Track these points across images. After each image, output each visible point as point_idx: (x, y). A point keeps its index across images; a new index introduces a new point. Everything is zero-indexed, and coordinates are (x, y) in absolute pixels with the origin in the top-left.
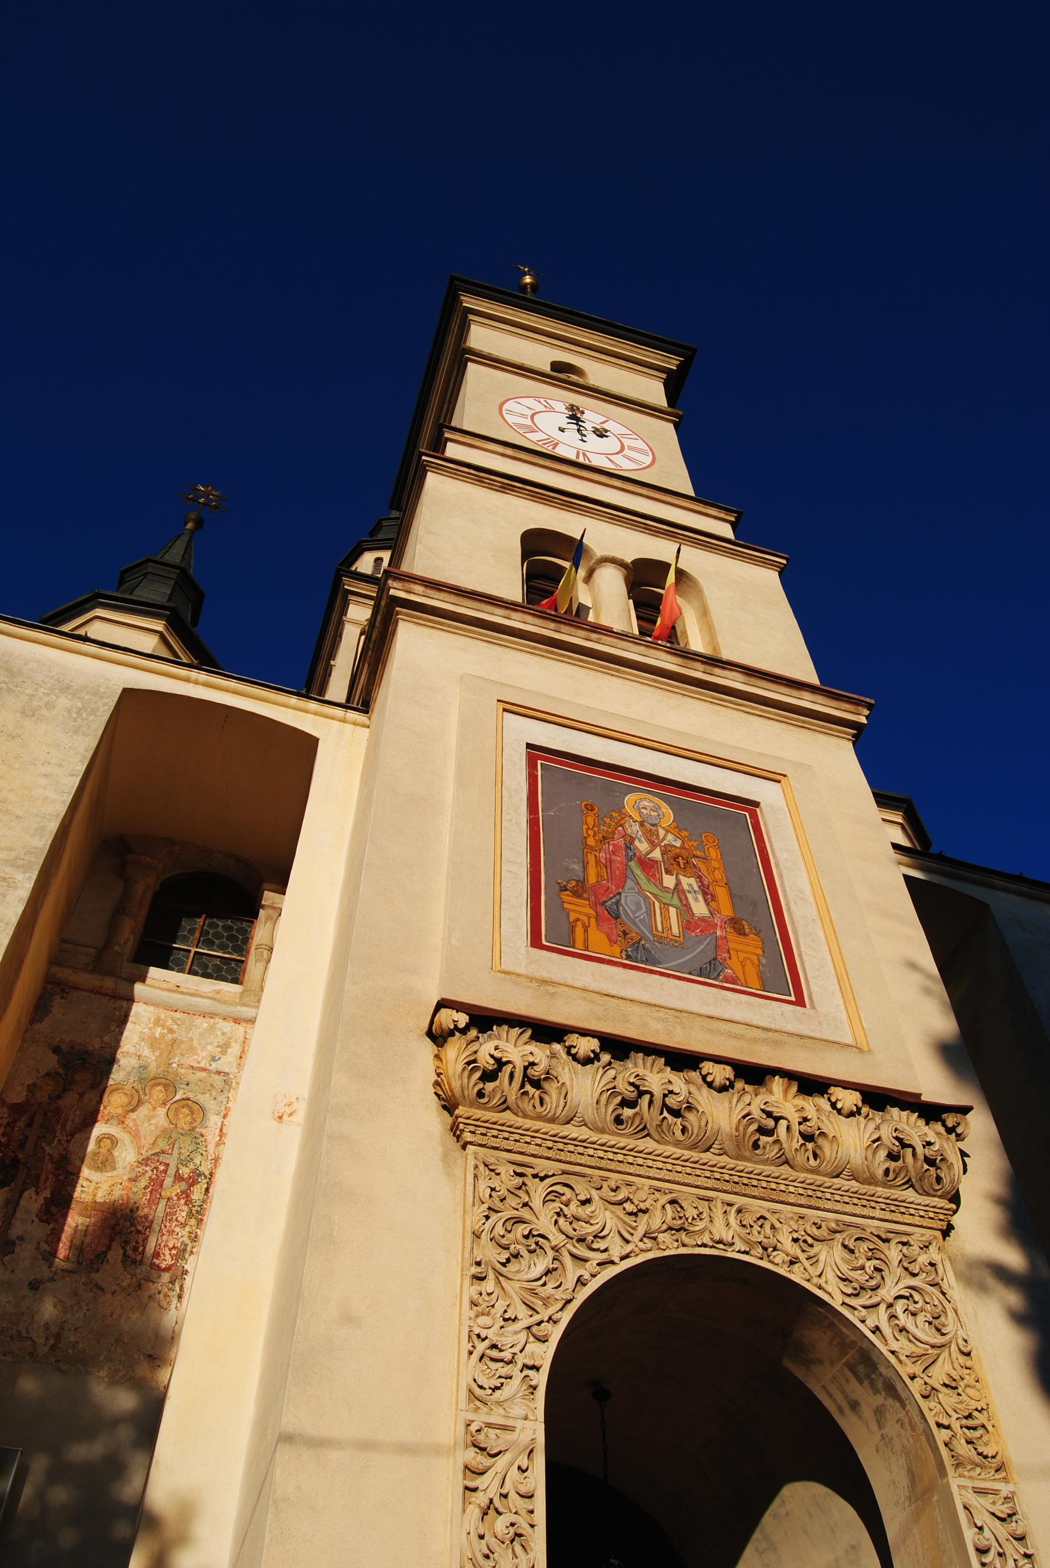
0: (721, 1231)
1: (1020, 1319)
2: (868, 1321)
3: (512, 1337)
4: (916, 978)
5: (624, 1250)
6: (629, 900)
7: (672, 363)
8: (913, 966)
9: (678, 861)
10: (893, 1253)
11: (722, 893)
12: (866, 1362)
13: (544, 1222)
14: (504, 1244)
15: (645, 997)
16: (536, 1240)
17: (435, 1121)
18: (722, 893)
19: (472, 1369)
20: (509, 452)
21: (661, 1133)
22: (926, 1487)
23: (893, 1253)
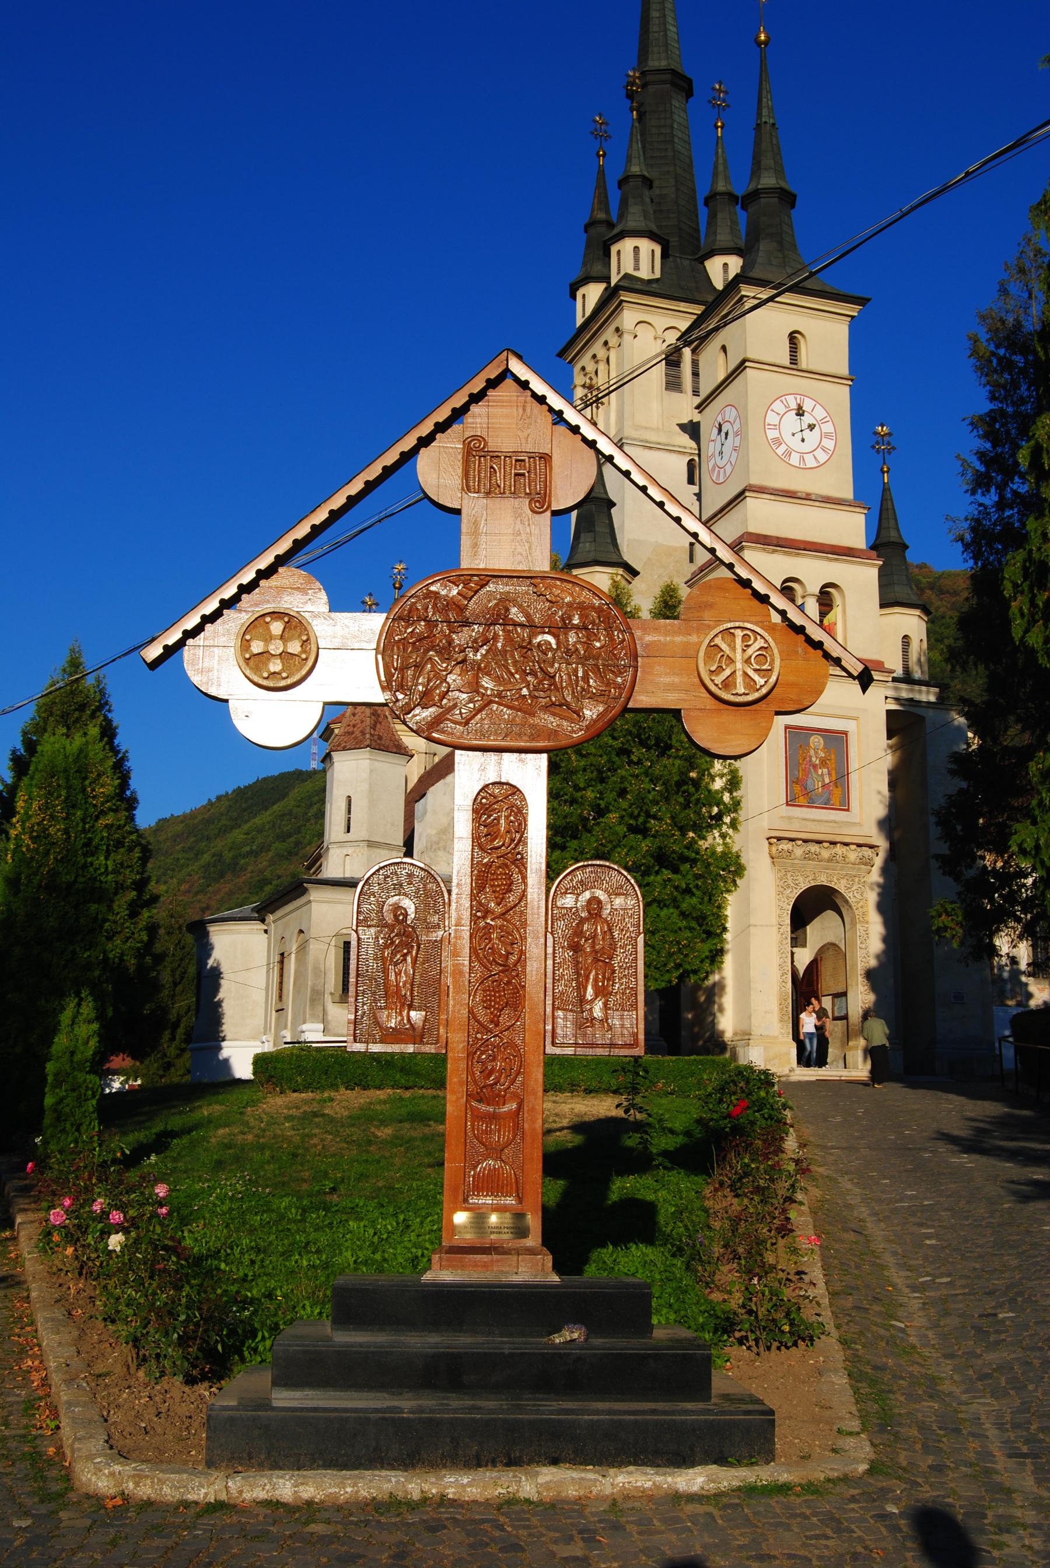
0: (823, 880)
1: (879, 894)
2: (848, 895)
3: (785, 906)
4: (879, 797)
5: (804, 886)
6: (809, 782)
7: (853, 310)
8: (879, 793)
9: (823, 763)
10: (857, 880)
11: (833, 772)
12: (847, 902)
13: (790, 882)
15: (812, 817)
16: (788, 886)
17: (769, 860)
18: (833, 772)
19: (778, 912)
20: (773, 497)
21: (813, 860)
22: (854, 923)
23: (857, 880)
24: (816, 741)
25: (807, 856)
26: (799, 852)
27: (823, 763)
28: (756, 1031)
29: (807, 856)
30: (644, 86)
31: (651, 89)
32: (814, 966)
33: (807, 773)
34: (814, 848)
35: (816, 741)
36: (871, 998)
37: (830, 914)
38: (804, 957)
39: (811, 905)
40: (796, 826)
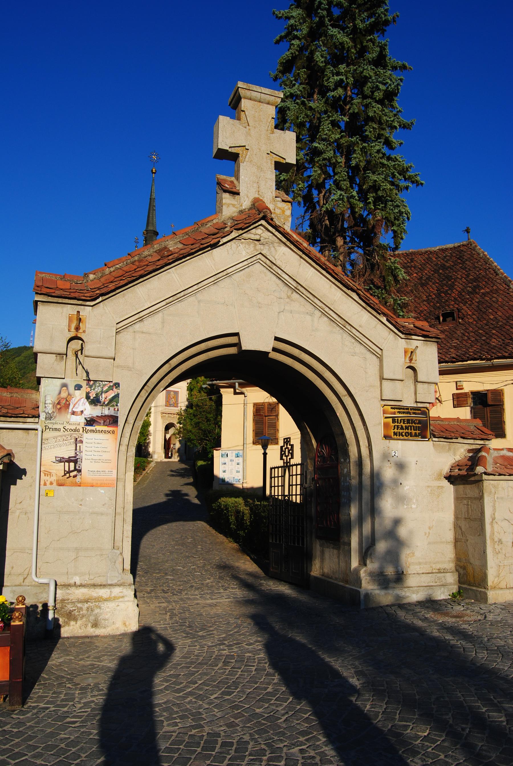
0: (172, 421)
9: (173, 398)
14: (163, 423)
24: (172, 393)
25: (169, 417)
26: (167, 416)
27: (173, 398)
28: (156, 451)
29: (169, 417)
30: (147, 233)
31: (149, 234)
32: (170, 438)
33: (170, 399)
34: (170, 415)
35: (172, 393)
36: (180, 445)
37: (173, 428)
38: (168, 436)
39: (168, 427)
40: (167, 410)
